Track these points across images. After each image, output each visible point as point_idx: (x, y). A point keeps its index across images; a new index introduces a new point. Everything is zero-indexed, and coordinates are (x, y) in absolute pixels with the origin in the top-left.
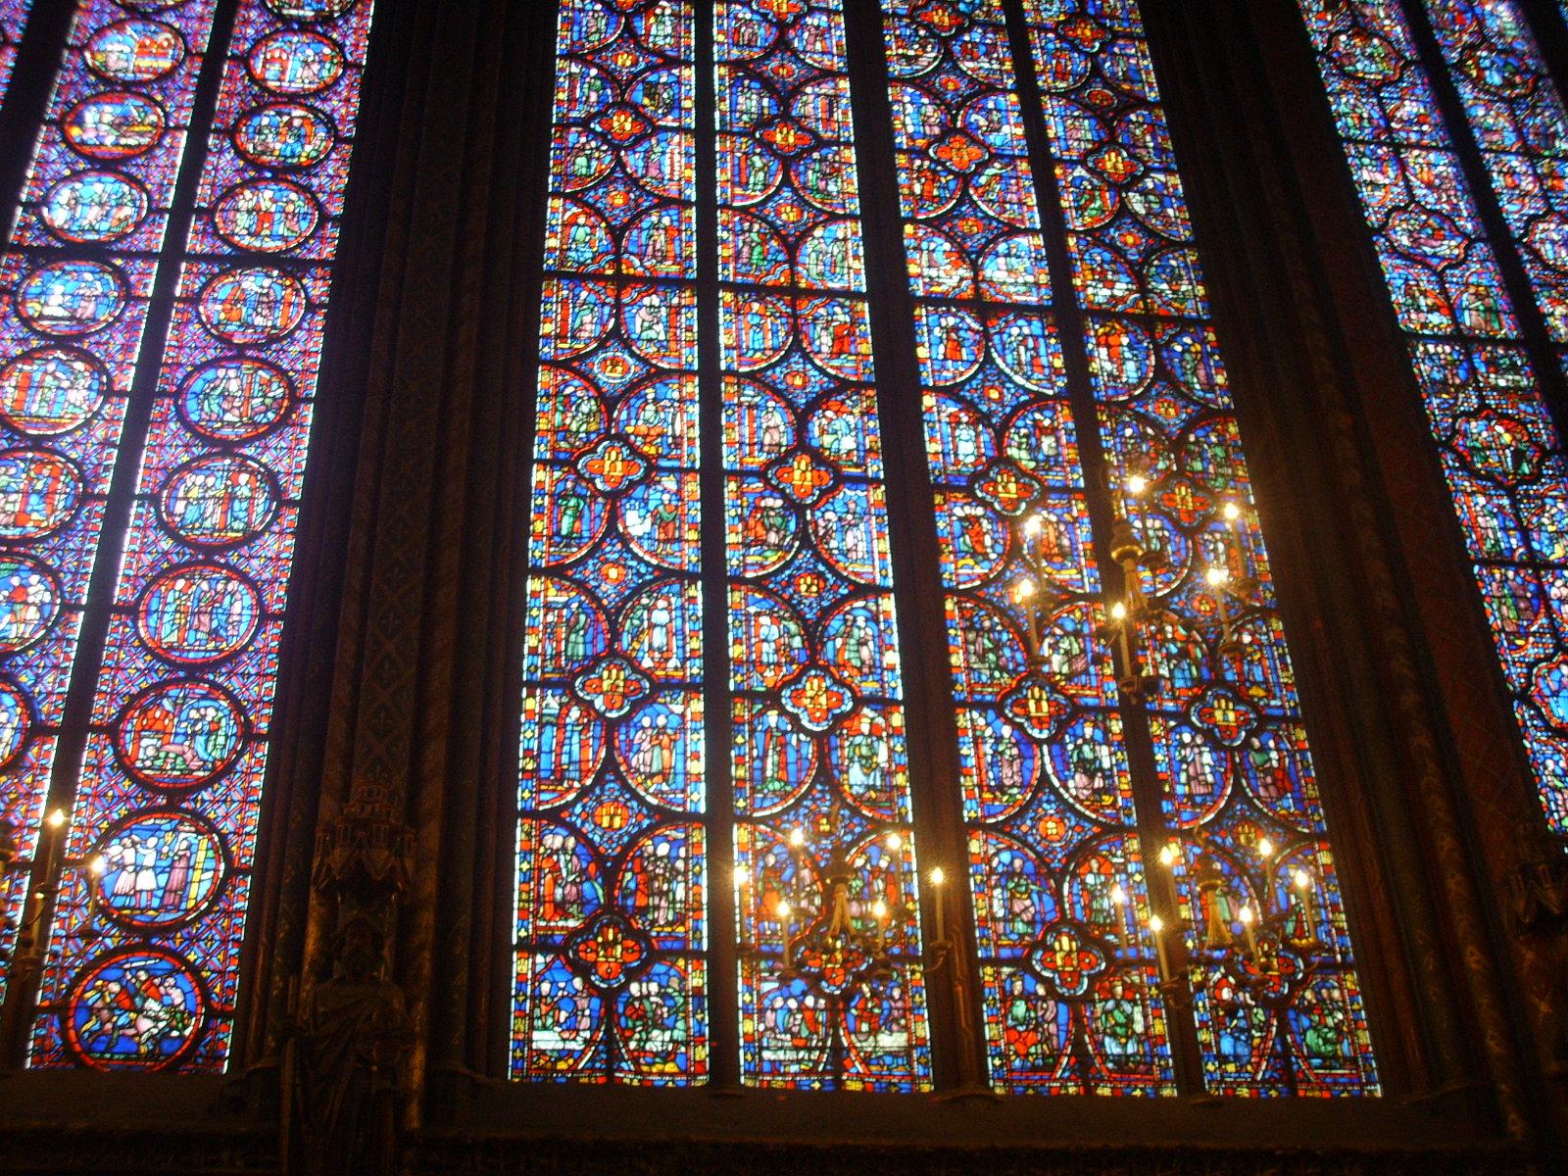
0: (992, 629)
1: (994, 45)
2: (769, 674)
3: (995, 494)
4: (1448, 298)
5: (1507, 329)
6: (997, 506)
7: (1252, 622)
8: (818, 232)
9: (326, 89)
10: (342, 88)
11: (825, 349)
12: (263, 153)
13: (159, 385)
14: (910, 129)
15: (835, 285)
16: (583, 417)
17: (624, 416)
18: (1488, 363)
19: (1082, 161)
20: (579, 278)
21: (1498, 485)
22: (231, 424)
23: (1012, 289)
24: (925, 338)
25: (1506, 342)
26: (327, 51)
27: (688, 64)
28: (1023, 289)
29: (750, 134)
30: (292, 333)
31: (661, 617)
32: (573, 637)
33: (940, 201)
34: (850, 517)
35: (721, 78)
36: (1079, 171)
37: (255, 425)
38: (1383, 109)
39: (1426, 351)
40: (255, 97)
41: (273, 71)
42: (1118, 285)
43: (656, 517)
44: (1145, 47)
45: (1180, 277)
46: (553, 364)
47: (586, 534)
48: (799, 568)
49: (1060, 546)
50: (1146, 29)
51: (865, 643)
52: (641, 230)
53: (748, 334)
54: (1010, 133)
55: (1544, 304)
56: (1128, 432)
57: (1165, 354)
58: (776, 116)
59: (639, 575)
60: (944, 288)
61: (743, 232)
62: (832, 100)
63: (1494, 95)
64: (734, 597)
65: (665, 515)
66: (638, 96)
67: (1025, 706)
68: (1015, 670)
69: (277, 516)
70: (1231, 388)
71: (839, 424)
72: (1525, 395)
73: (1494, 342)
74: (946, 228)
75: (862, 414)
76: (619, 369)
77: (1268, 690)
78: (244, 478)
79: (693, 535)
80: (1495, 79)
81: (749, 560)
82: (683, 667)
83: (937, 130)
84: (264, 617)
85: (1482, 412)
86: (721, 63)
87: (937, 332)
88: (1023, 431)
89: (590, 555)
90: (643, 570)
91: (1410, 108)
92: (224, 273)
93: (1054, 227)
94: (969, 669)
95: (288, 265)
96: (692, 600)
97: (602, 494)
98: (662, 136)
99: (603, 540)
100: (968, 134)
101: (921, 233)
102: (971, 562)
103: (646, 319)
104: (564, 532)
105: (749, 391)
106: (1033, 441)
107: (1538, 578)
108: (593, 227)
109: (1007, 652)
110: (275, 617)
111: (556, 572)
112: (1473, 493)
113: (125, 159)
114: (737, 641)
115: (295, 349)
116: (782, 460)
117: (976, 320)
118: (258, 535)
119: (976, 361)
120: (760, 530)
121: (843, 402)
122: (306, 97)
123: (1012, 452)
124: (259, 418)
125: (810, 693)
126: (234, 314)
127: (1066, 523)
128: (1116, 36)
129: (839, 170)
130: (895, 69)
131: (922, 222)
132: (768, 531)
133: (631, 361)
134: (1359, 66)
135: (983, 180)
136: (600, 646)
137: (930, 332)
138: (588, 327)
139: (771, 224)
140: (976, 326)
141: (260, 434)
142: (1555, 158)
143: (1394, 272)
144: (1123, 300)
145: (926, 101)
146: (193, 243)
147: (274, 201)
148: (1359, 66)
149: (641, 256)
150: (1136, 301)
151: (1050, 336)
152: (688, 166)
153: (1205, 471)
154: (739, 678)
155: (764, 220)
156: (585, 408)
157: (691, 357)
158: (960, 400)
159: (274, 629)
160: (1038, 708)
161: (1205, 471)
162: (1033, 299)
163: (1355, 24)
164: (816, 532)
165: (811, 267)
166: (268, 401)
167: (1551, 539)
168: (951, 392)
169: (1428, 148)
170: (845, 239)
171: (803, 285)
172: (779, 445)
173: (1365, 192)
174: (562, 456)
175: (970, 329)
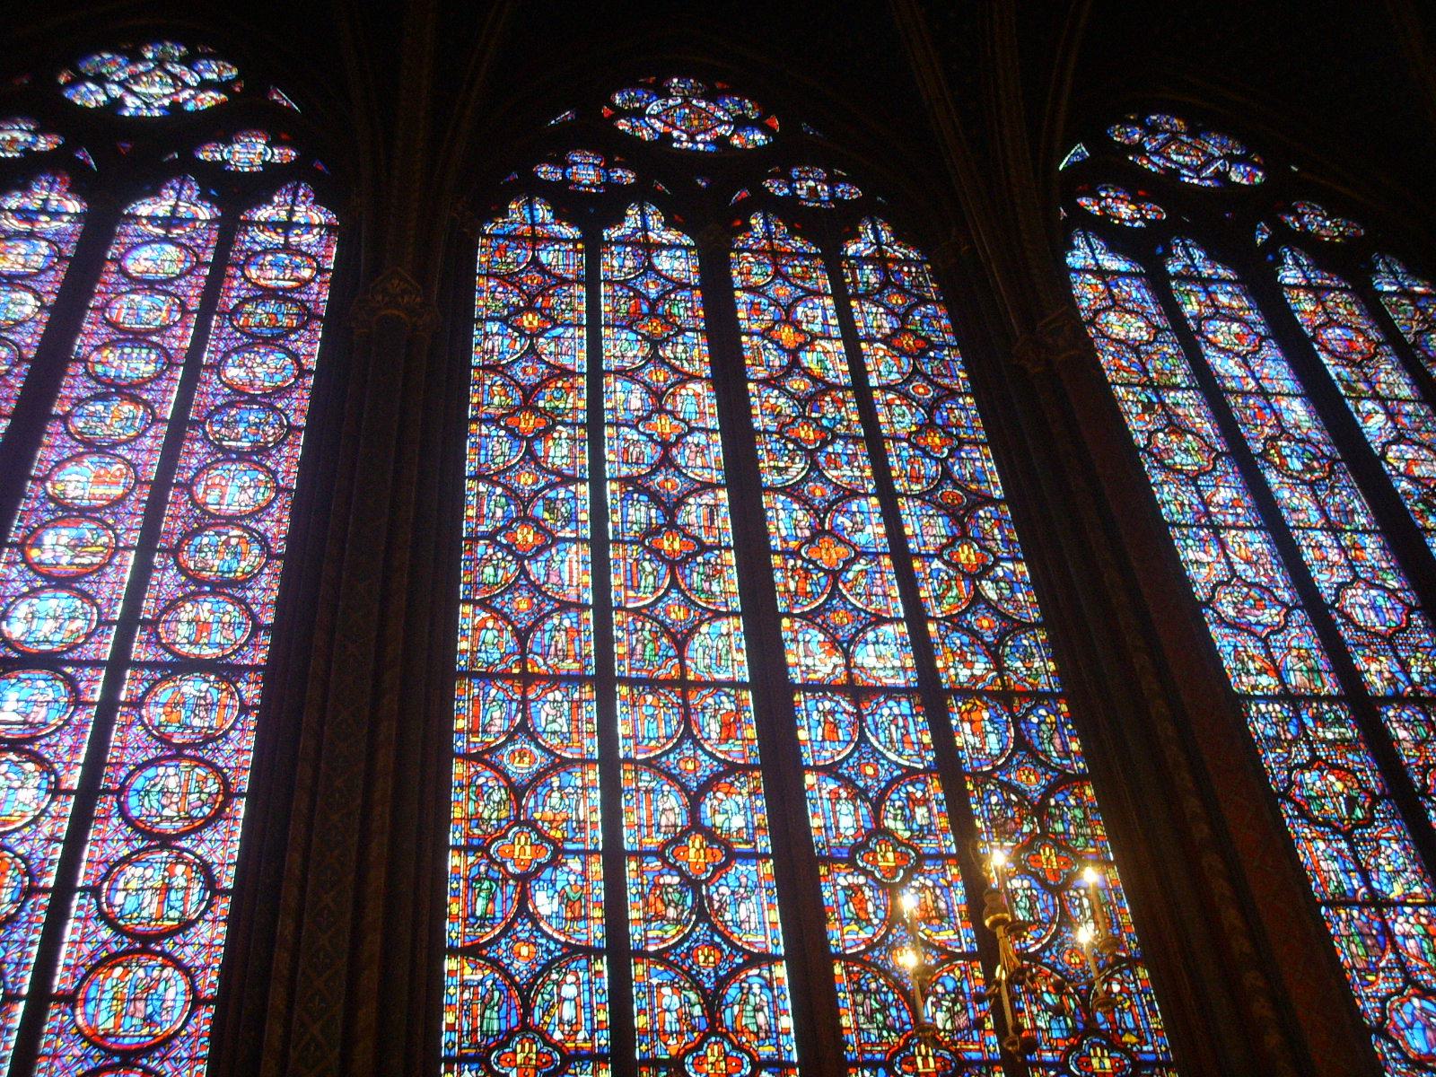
0: (878, 991)
1: (855, 455)
2: (672, 1042)
3: (875, 863)
4: (1273, 661)
5: (1329, 686)
6: (878, 875)
7: (1120, 972)
8: (704, 628)
9: (260, 512)
10: (274, 510)
11: (714, 736)
12: (203, 569)
13: (103, 783)
14: (784, 533)
15: (722, 676)
16: (494, 805)
17: (531, 803)
18: (1315, 718)
19: (939, 555)
20: (488, 677)
21: (1336, 831)
22: (170, 819)
23: (881, 673)
24: (805, 722)
25: (1330, 699)
26: (261, 477)
27: (582, 481)
28: (891, 673)
29: (641, 543)
30: (226, 734)
31: (569, 991)
32: (488, 1013)
33: (812, 596)
34: (742, 890)
35: (613, 493)
36: (937, 564)
37: (192, 819)
38: (1201, 496)
39: (1259, 711)
40: (197, 519)
41: (212, 497)
42: (977, 665)
43: (563, 896)
44: (988, 451)
45: (1032, 654)
46: (467, 757)
47: (499, 915)
48: (696, 941)
49: (937, 909)
50: (988, 436)
51: (761, 1009)
52: (544, 631)
53: (644, 724)
54: (872, 533)
55: (1359, 662)
56: (994, 799)
57: (1023, 726)
58: (662, 526)
59: (548, 951)
60: (819, 675)
61: (636, 631)
62: (713, 510)
63: (1296, 479)
64: (638, 970)
65: (571, 895)
66: (539, 511)
67: (914, 1063)
68: (901, 1029)
69: (210, 904)
70: (1085, 754)
71: (729, 805)
72: (1350, 745)
73: (1319, 698)
74: (819, 620)
75: (750, 794)
76: (526, 760)
77: (1139, 1037)
78: (180, 869)
79: (598, 913)
80: (1296, 465)
81: (651, 934)
82: (591, 1038)
83: (807, 533)
84: (197, 1002)
85: (1313, 763)
86: (613, 480)
87: (815, 715)
88: (898, 803)
89: (503, 934)
90: (552, 946)
91: (1224, 495)
92: (165, 679)
93: (916, 615)
94: (859, 1030)
95: (224, 670)
96: (599, 973)
97: (514, 876)
98: (561, 546)
99: (514, 920)
100: (836, 535)
101: (797, 625)
102: (856, 928)
103: (550, 713)
104: (478, 913)
105: (646, 777)
106: (907, 811)
108: (501, 630)
109: (893, 1012)
110: (207, 1002)
111: (472, 952)
112: (1314, 838)
113: (77, 577)
114: (641, 1011)
115: (229, 748)
116: (678, 840)
117: (849, 702)
118: (192, 923)
119: (852, 741)
120: (660, 906)
121: (732, 784)
122: (242, 518)
123: (889, 823)
124: (195, 813)
125: (711, 1059)
126: (174, 716)
127: (942, 888)
128: (962, 442)
129: (721, 572)
130: (767, 479)
131: (797, 615)
132: (667, 907)
133: (537, 752)
134: (1177, 459)
135: (850, 575)
136: (514, 1021)
137: (808, 716)
138: (498, 722)
139: (662, 623)
140: (851, 709)
141: (195, 828)
142: (1356, 531)
143: (1223, 641)
144: (982, 678)
145: (796, 506)
146: (138, 652)
147: (212, 612)
148: (1177, 459)
149: (544, 656)
150: (994, 679)
151: (918, 714)
152: (585, 572)
153: (1066, 832)
154: (644, 1047)
155: (655, 619)
156: (496, 797)
157: (592, 747)
158: (839, 777)
159: (206, 1013)
160: (926, 1064)
161: (1066, 832)
162: (901, 682)
163: (1170, 423)
164: (710, 905)
165: (699, 659)
166: (204, 797)
167: (1389, 879)
168: (831, 770)
169: (1243, 528)
170: (728, 635)
171: (691, 677)
172: (675, 826)
173: (1192, 571)
174: (475, 842)
175: (845, 711)
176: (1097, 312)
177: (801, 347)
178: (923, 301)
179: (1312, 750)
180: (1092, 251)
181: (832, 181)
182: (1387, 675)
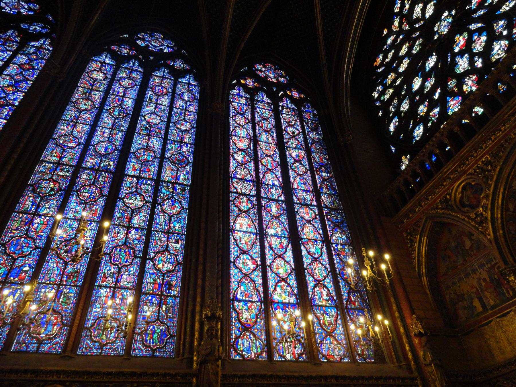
5: (74, 163)
72: (66, 177)
73: (67, 165)
80: (117, 113)
85: (51, 179)
107: (33, 217)
176: (92, 71)
178: (41, 59)
180: (106, 57)
181: (42, 28)
182: (94, 163)
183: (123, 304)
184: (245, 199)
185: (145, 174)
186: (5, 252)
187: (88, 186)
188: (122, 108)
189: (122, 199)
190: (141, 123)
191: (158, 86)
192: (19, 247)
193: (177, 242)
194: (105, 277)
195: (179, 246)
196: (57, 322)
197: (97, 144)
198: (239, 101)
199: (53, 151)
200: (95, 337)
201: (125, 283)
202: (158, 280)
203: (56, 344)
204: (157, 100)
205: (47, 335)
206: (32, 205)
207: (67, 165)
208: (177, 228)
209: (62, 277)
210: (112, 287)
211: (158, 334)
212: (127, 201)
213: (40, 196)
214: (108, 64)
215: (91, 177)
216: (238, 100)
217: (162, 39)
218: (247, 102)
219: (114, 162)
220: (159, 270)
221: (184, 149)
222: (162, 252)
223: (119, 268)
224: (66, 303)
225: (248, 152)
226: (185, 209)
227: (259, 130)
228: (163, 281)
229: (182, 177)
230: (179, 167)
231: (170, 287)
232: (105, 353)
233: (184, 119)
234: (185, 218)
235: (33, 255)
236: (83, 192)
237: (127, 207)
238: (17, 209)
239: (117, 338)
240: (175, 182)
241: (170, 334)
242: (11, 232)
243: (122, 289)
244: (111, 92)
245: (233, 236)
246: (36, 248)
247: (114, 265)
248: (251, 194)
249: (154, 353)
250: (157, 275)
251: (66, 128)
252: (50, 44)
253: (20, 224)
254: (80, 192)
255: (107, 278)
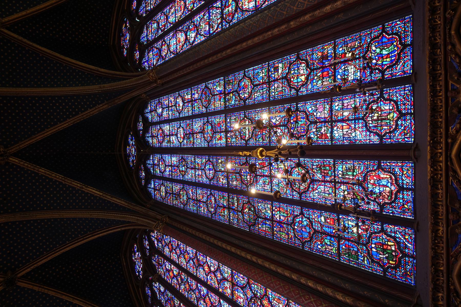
5: (226, 195)
19: (207, 276)
36: (208, 277)
72: (238, 200)
73: (229, 201)
80: (183, 168)
85: (242, 212)
107: (275, 221)
128: (186, 250)
153: (260, 293)
167: (267, 213)
177: (173, 273)
179: (240, 212)
183: (349, 107)
184: (226, 11)
185: (222, 126)
186: (310, 241)
187: (241, 178)
188: (179, 164)
189: (246, 141)
190: (186, 144)
191: (158, 138)
192: (303, 229)
193: (276, 69)
194: (321, 137)
195: (280, 65)
196: (375, 176)
197: (208, 179)
198: (152, 59)
199: (220, 215)
200: (391, 127)
201: (326, 112)
202: (318, 75)
203: (401, 169)
204: (167, 135)
205: (392, 184)
206: (266, 224)
207: (229, 201)
208: (263, 74)
209: (327, 181)
210: (331, 125)
211: (381, 50)
212: (247, 136)
213: (257, 218)
214: (154, 184)
215: (234, 177)
216: (151, 60)
217: (129, 146)
218: (150, 51)
219: (219, 159)
220: (307, 79)
221: (196, 96)
222: (289, 81)
223: (310, 124)
224: (354, 171)
225: (186, 28)
226: (244, 73)
227: (168, 27)
228: (319, 68)
229: (218, 89)
230: (211, 95)
231: (324, 57)
232: (411, 109)
233: (175, 105)
234: (253, 70)
235: (309, 214)
236: (247, 180)
237: (252, 135)
238: (270, 237)
239: (391, 100)
240: (225, 94)
241: (381, 33)
242: (291, 239)
243: (332, 114)
244: (171, 177)
245: (262, 6)
246: (302, 214)
247: (308, 130)
248: (220, 6)
249: (408, 45)
250: (313, 79)
251: (203, 208)
252: (154, 233)
253: (282, 232)
254: (248, 183)
255: (322, 133)
